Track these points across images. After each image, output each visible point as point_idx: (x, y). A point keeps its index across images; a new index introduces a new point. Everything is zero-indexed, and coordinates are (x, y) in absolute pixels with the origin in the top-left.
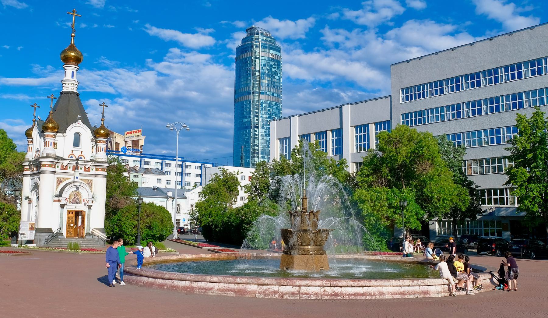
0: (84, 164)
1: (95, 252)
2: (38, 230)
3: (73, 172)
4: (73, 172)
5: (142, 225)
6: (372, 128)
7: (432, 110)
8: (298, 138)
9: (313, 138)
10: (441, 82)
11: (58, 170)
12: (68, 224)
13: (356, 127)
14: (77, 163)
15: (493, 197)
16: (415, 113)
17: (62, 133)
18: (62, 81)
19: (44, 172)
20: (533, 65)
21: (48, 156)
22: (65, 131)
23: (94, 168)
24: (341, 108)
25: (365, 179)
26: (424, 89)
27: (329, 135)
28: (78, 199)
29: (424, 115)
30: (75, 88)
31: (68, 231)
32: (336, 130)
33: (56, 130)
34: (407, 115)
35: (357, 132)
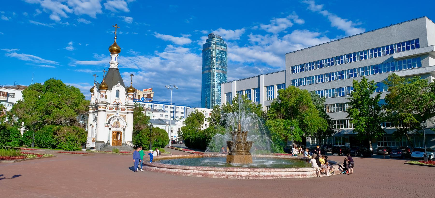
2: (97, 142)
5: (153, 139)
6: (276, 87)
7: (308, 78)
8: (236, 93)
9: (244, 93)
10: (313, 63)
11: (107, 110)
12: (113, 139)
13: (267, 87)
14: (118, 106)
15: (340, 124)
16: (299, 79)
19: (100, 111)
20: (362, 54)
21: (102, 103)
22: (111, 89)
23: (127, 109)
24: (259, 77)
25: (272, 115)
26: (303, 67)
27: (253, 91)
29: (303, 80)
31: (113, 142)
32: (256, 88)
34: (294, 80)
35: (267, 90)
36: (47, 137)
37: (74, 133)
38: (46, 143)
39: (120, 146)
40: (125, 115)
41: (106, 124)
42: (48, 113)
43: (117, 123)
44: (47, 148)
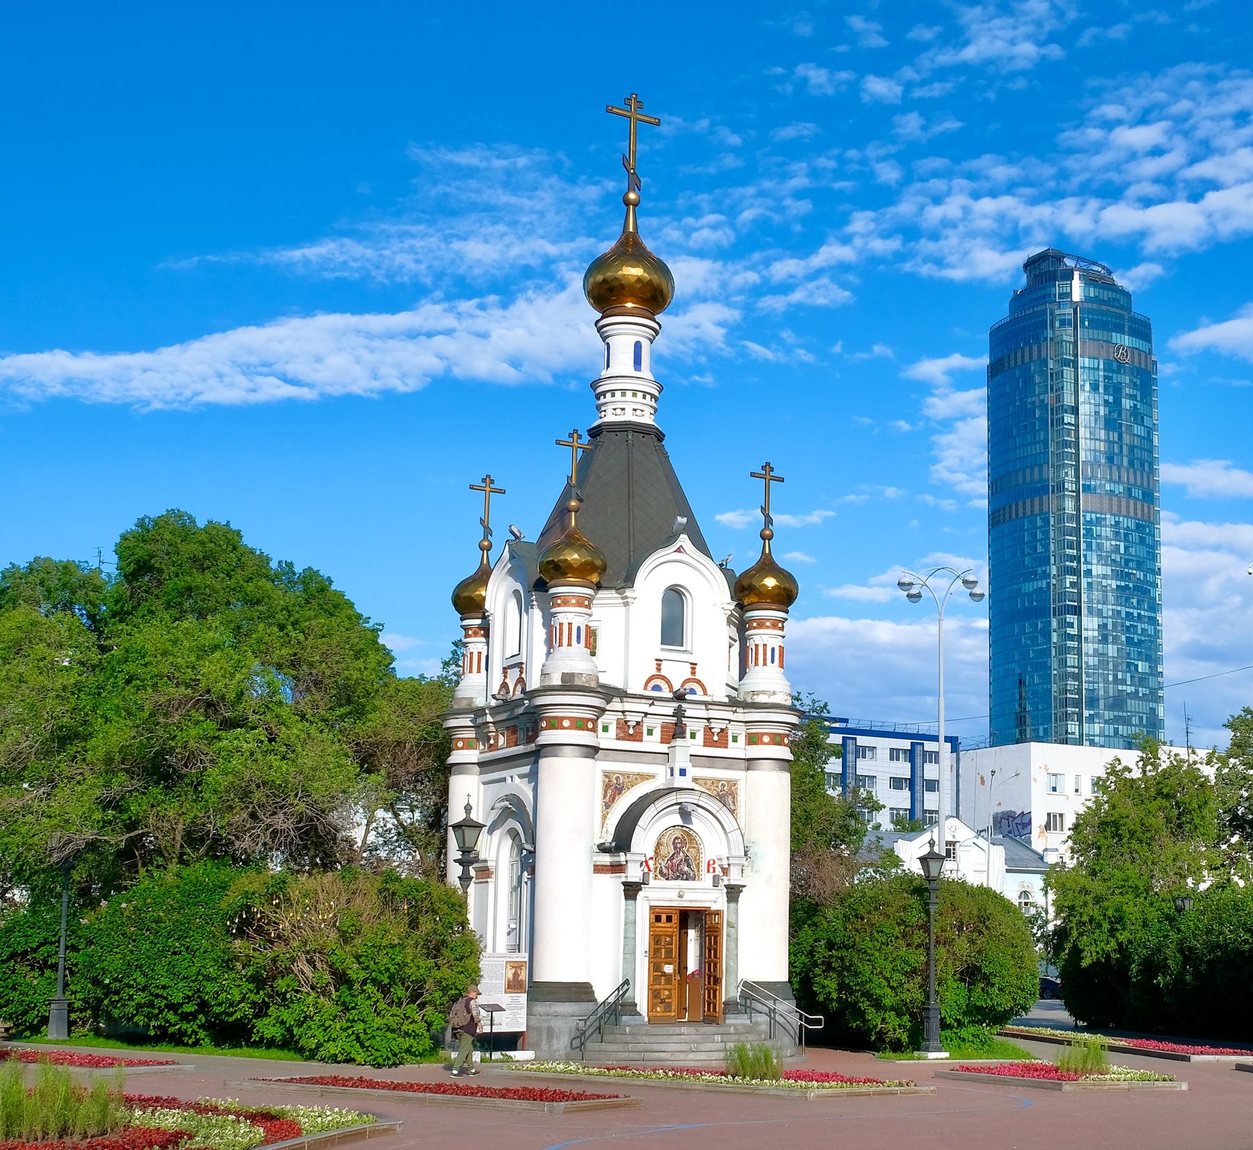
0: (704, 714)
1: (856, 1088)
2: (539, 992)
3: (664, 748)
4: (664, 748)
5: (946, 964)
11: (607, 740)
12: (655, 967)
14: (679, 713)
17: (619, 590)
18: (594, 385)
21: (569, 684)
22: (629, 581)
23: (741, 731)
30: (648, 410)
31: (654, 995)
33: (595, 578)
36: (182, 962)
37: (396, 929)
38: (172, 1007)
39: (711, 1019)
40: (733, 783)
41: (603, 849)
42: (160, 770)
43: (678, 844)
44: (177, 1040)
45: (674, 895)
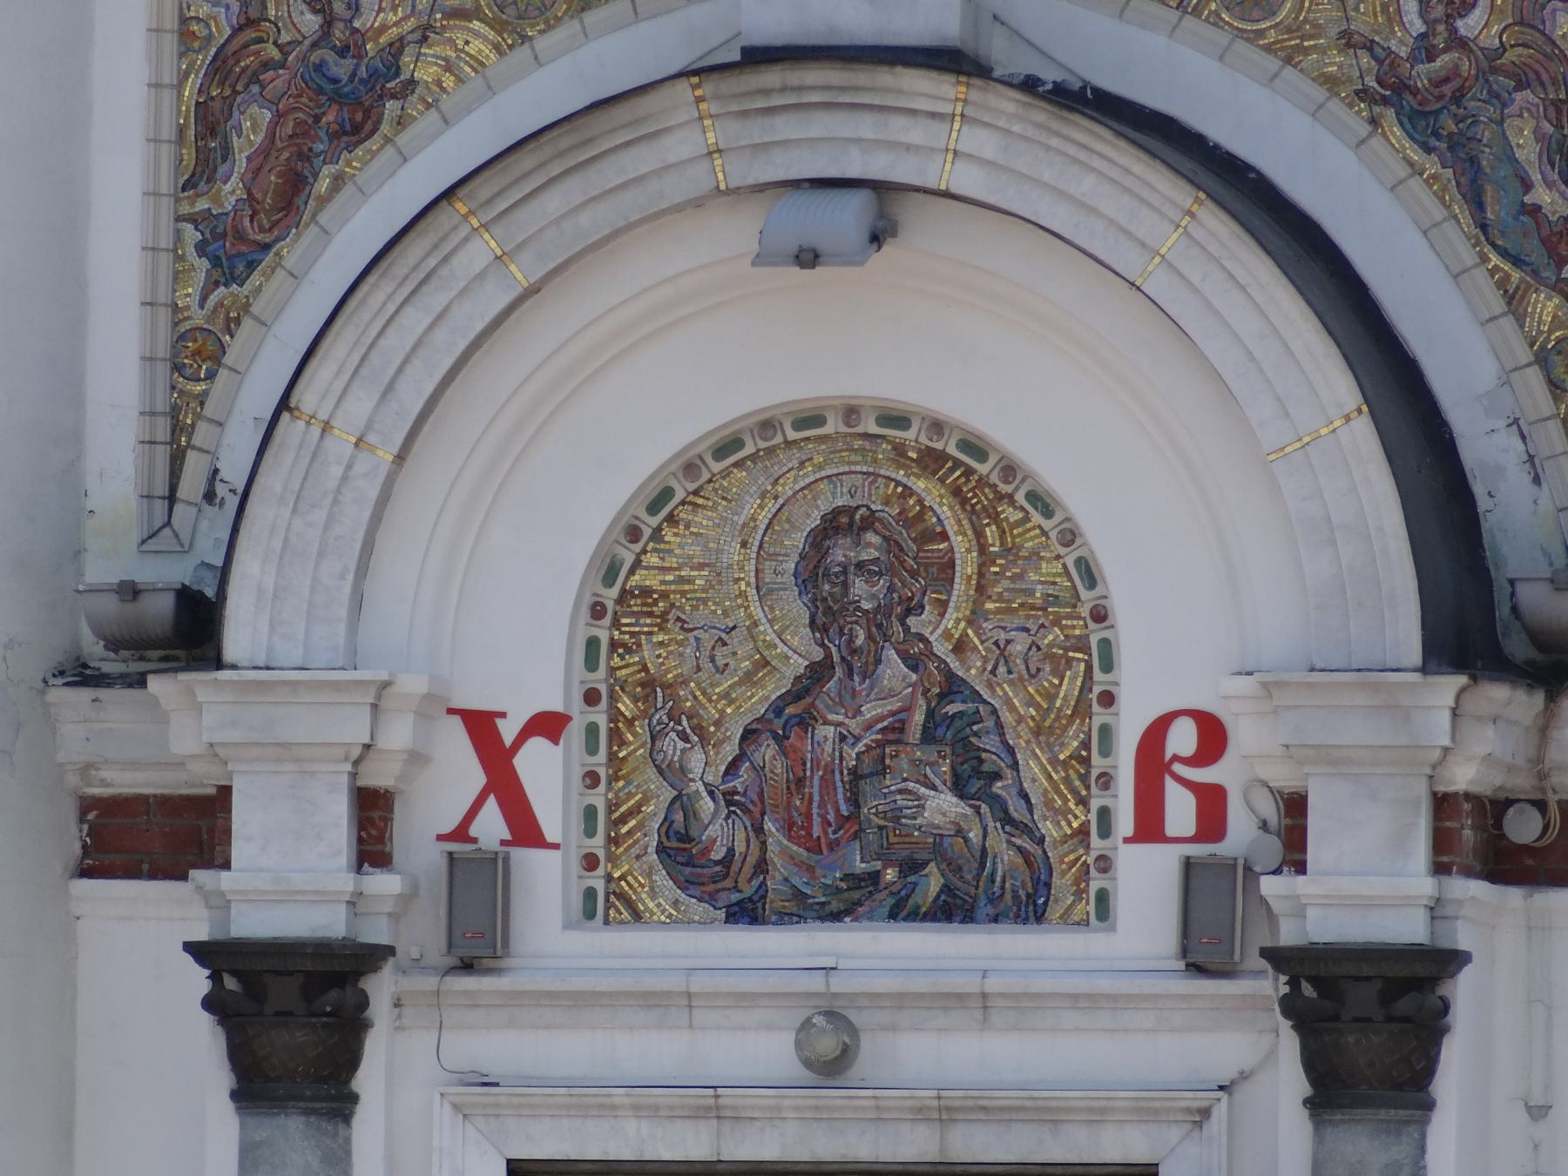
28: (960, 739)
45: (766, 1050)
